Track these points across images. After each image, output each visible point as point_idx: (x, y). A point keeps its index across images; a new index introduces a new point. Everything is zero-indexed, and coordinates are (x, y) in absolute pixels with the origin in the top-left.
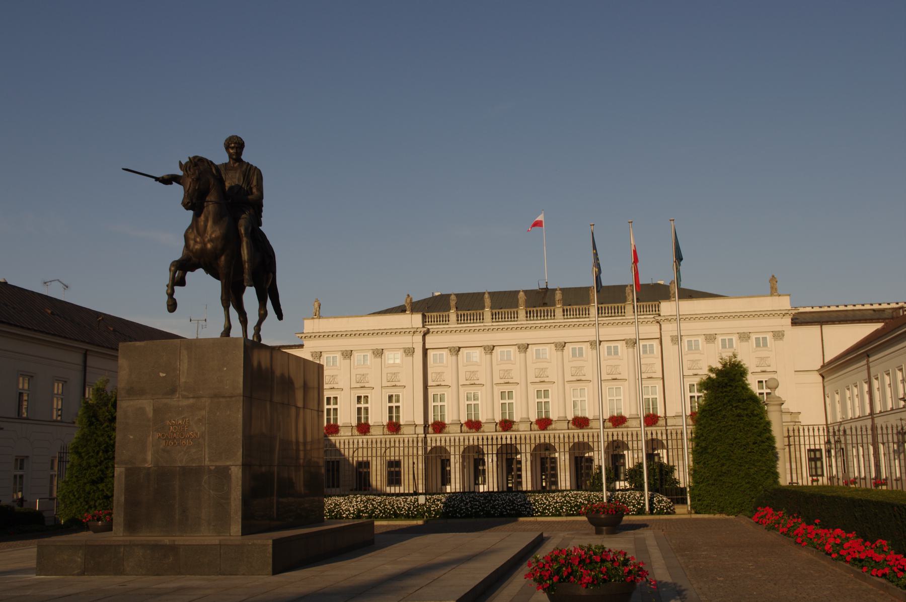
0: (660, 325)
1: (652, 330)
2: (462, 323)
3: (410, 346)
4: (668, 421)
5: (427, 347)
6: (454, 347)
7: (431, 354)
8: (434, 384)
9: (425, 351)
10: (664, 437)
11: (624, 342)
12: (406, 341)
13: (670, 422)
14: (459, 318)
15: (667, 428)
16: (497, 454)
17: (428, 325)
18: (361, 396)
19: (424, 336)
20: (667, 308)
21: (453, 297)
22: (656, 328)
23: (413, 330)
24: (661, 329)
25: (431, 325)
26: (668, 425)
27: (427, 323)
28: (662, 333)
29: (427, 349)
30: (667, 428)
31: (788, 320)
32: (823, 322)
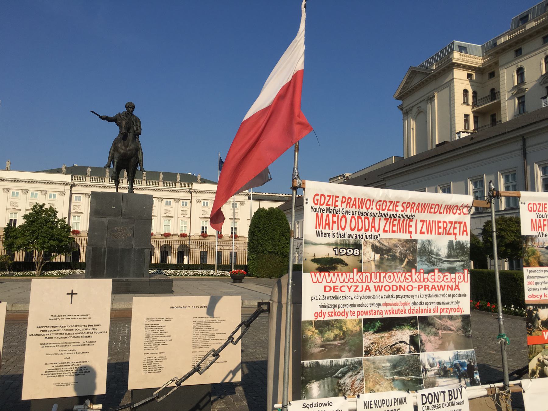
0: (192, 194)
1: (188, 196)
3: (63, 191)
5: (72, 192)
6: (88, 194)
7: (74, 196)
8: (74, 211)
9: (71, 194)
10: (188, 244)
11: (157, 199)
12: (61, 188)
14: (92, 180)
19: (71, 187)
20: (196, 186)
21: (89, 169)
22: (189, 195)
23: (65, 183)
25: (76, 181)
27: (73, 180)
31: (247, 197)
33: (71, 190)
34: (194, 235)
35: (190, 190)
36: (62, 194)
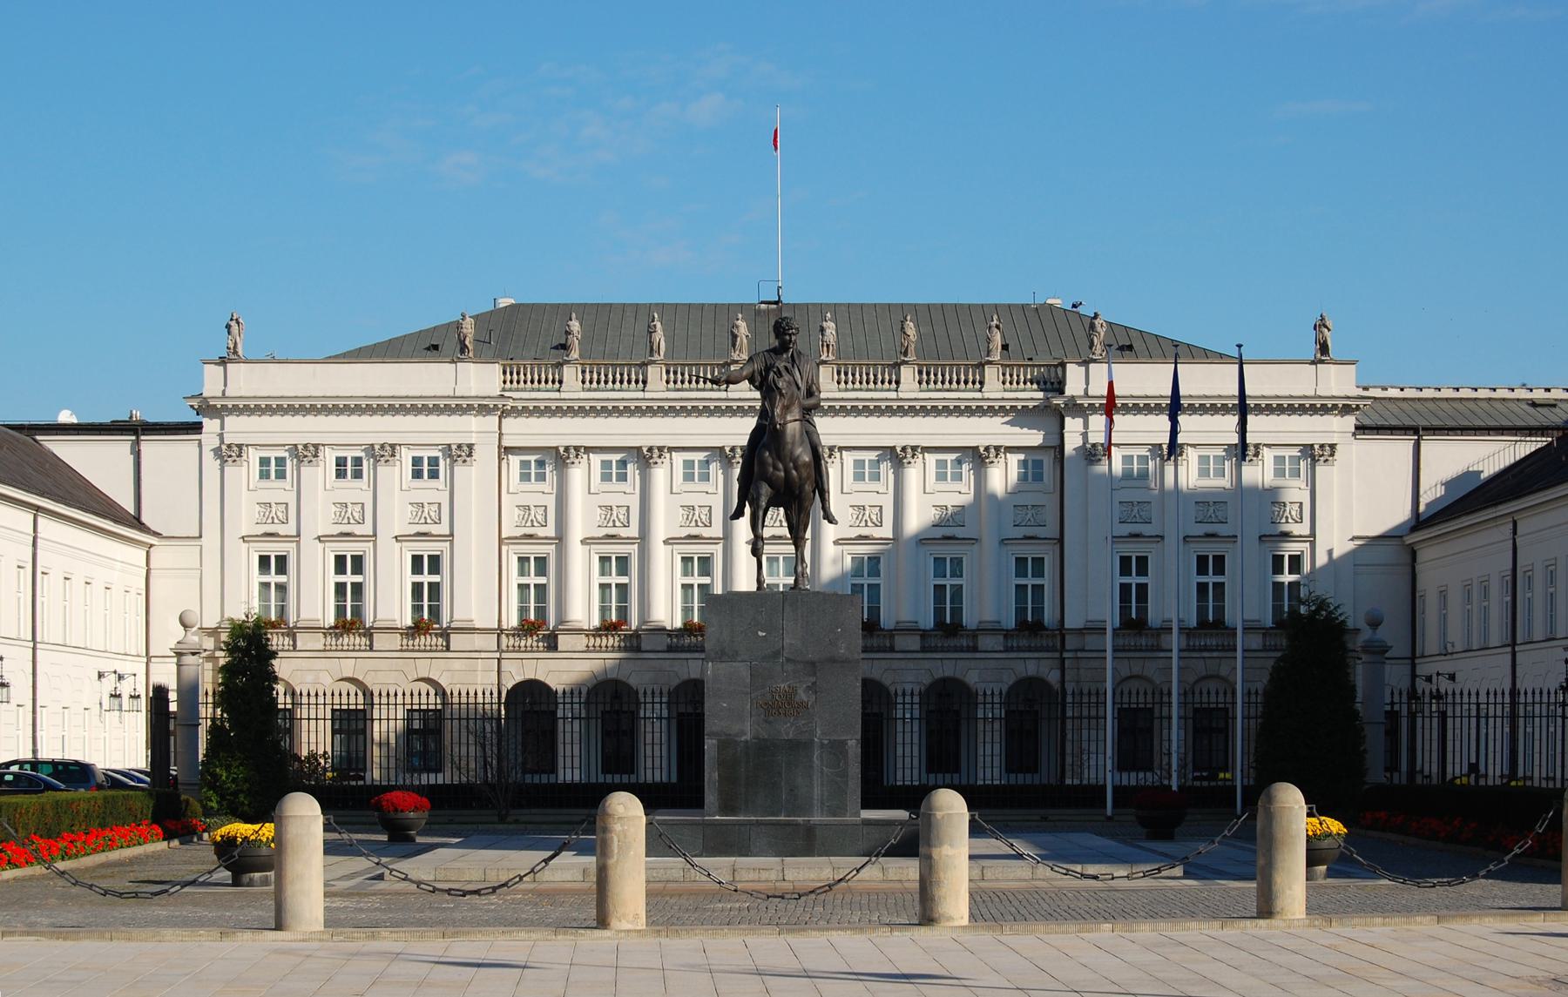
2: (595, 390)
4: (1067, 637)
5: (505, 443)
9: (506, 451)
13: (1071, 642)
15: (1066, 655)
16: (669, 703)
17: (510, 390)
18: (344, 557)
24: (1062, 426)
25: (517, 390)
26: (1067, 647)
28: (1066, 435)
29: (509, 450)
30: (1066, 655)
31: (1350, 422)
32: (1425, 429)
33: (501, 434)
34: (1080, 632)
35: (1058, 401)
36: (461, 453)
